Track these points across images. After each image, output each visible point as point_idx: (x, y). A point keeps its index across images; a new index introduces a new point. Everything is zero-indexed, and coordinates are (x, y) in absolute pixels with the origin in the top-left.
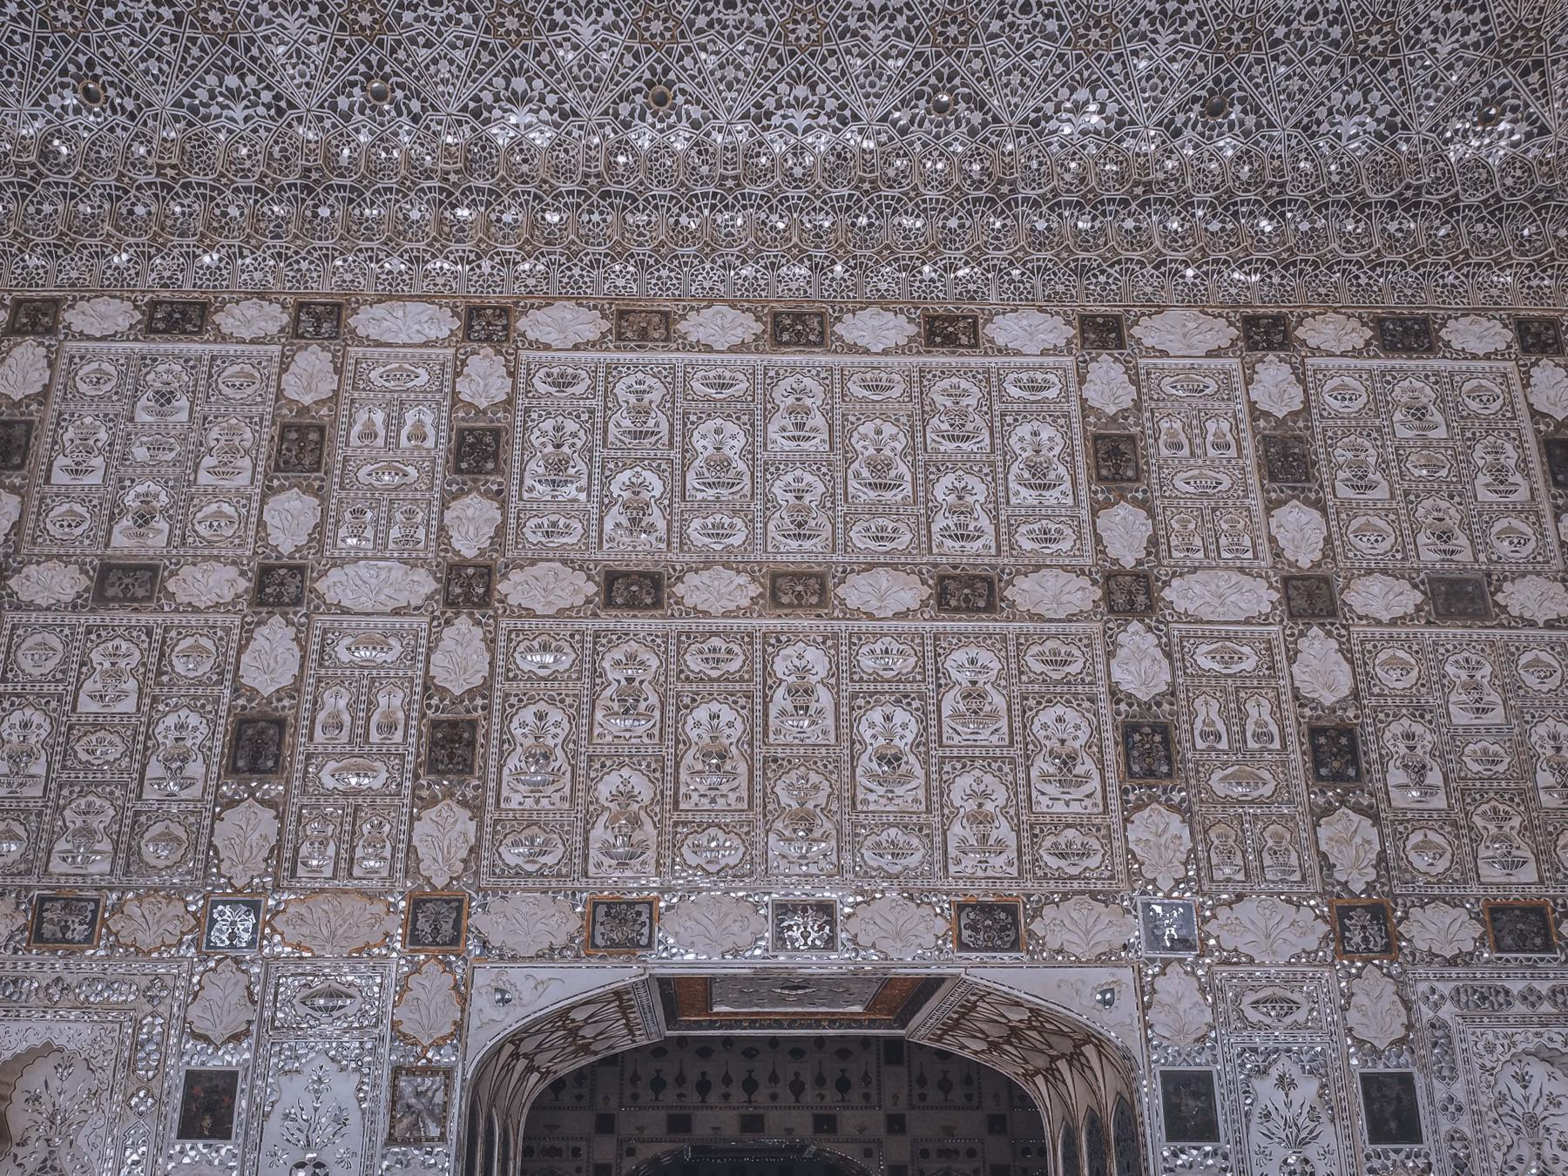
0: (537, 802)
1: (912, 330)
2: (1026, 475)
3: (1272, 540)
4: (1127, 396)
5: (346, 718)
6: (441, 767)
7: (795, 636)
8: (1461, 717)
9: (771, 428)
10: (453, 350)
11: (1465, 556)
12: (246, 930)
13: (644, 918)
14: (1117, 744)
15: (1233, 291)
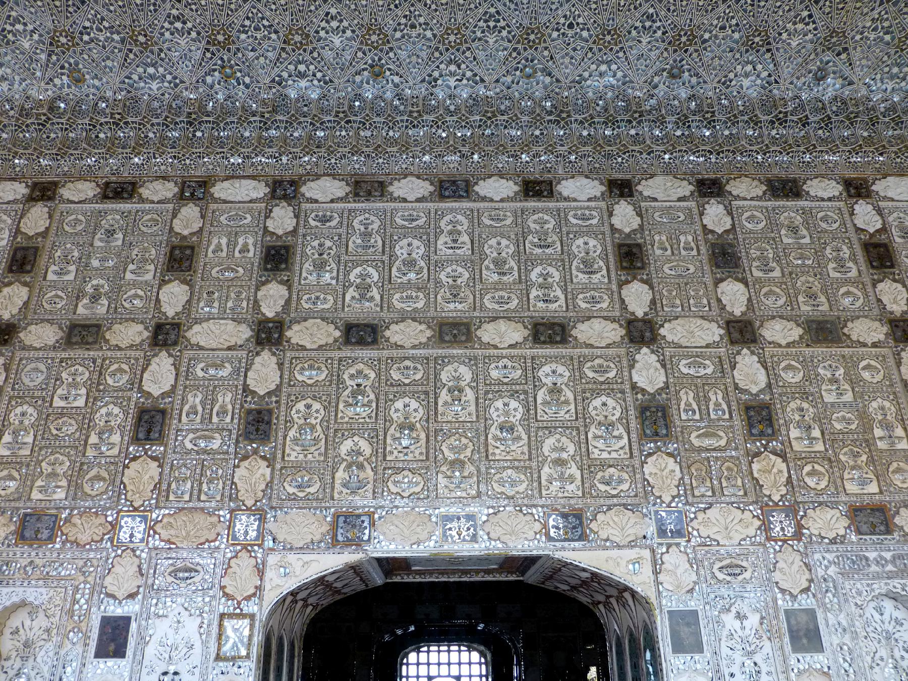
0: (306, 456)
1: (516, 188)
2: (582, 266)
3: (719, 301)
4: (636, 222)
5: (200, 409)
6: (252, 437)
8: (829, 398)
9: (439, 242)
10: (265, 204)
11: (825, 307)
12: (139, 532)
13: (366, 524)
14: (636, 418)
15: (691, 166)
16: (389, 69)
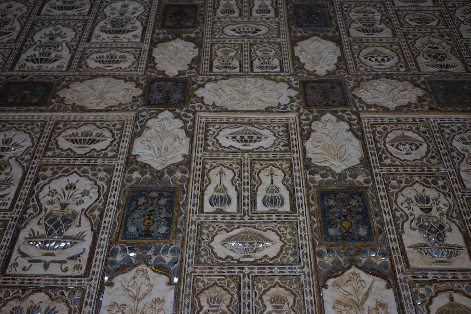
14: (119, 206)
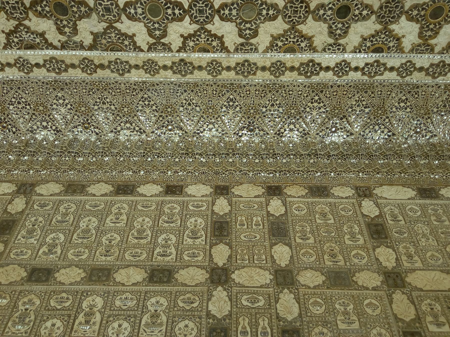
1: (161, 189)
2: (190, 234)
3: (272, 257)
7: (94, 292)
9: (108, 219)
10: (11, 197)
11: (342, 263)
15: (264, 179)
16: (93, 125)
